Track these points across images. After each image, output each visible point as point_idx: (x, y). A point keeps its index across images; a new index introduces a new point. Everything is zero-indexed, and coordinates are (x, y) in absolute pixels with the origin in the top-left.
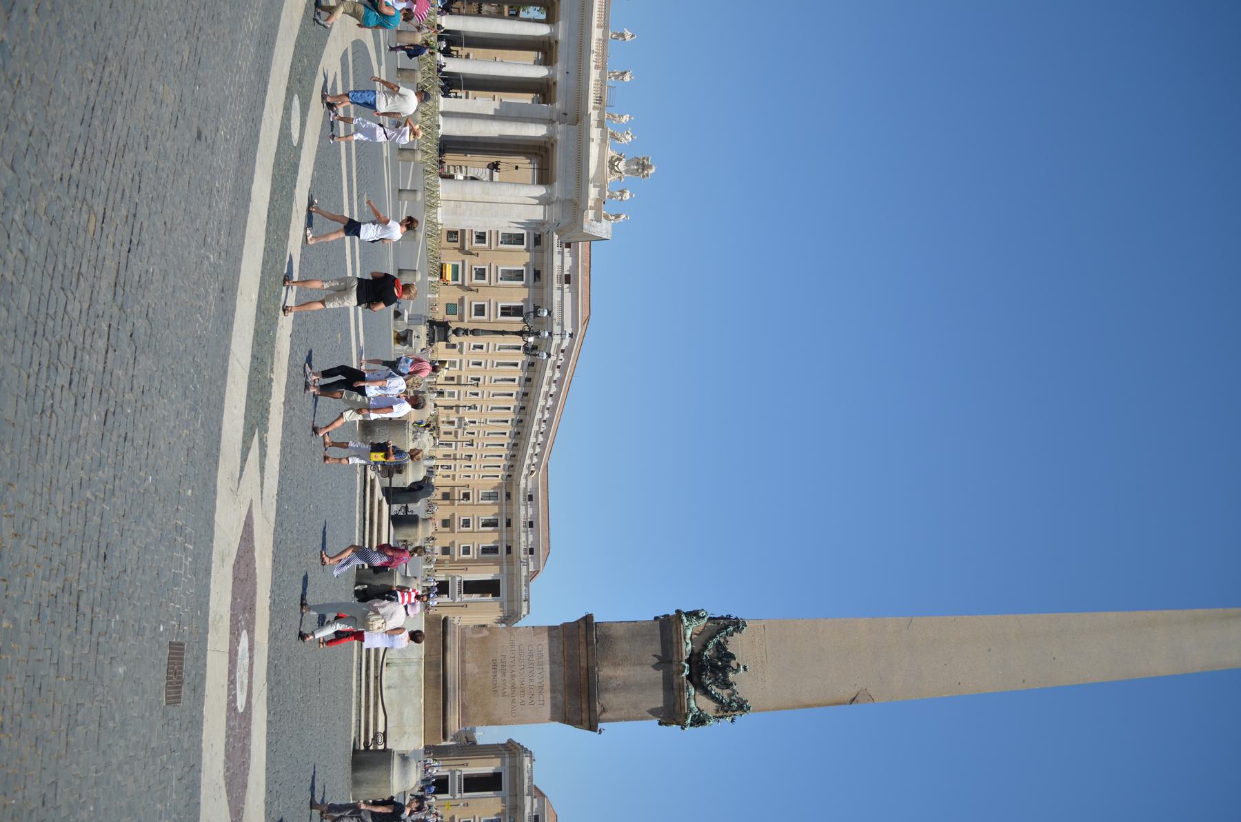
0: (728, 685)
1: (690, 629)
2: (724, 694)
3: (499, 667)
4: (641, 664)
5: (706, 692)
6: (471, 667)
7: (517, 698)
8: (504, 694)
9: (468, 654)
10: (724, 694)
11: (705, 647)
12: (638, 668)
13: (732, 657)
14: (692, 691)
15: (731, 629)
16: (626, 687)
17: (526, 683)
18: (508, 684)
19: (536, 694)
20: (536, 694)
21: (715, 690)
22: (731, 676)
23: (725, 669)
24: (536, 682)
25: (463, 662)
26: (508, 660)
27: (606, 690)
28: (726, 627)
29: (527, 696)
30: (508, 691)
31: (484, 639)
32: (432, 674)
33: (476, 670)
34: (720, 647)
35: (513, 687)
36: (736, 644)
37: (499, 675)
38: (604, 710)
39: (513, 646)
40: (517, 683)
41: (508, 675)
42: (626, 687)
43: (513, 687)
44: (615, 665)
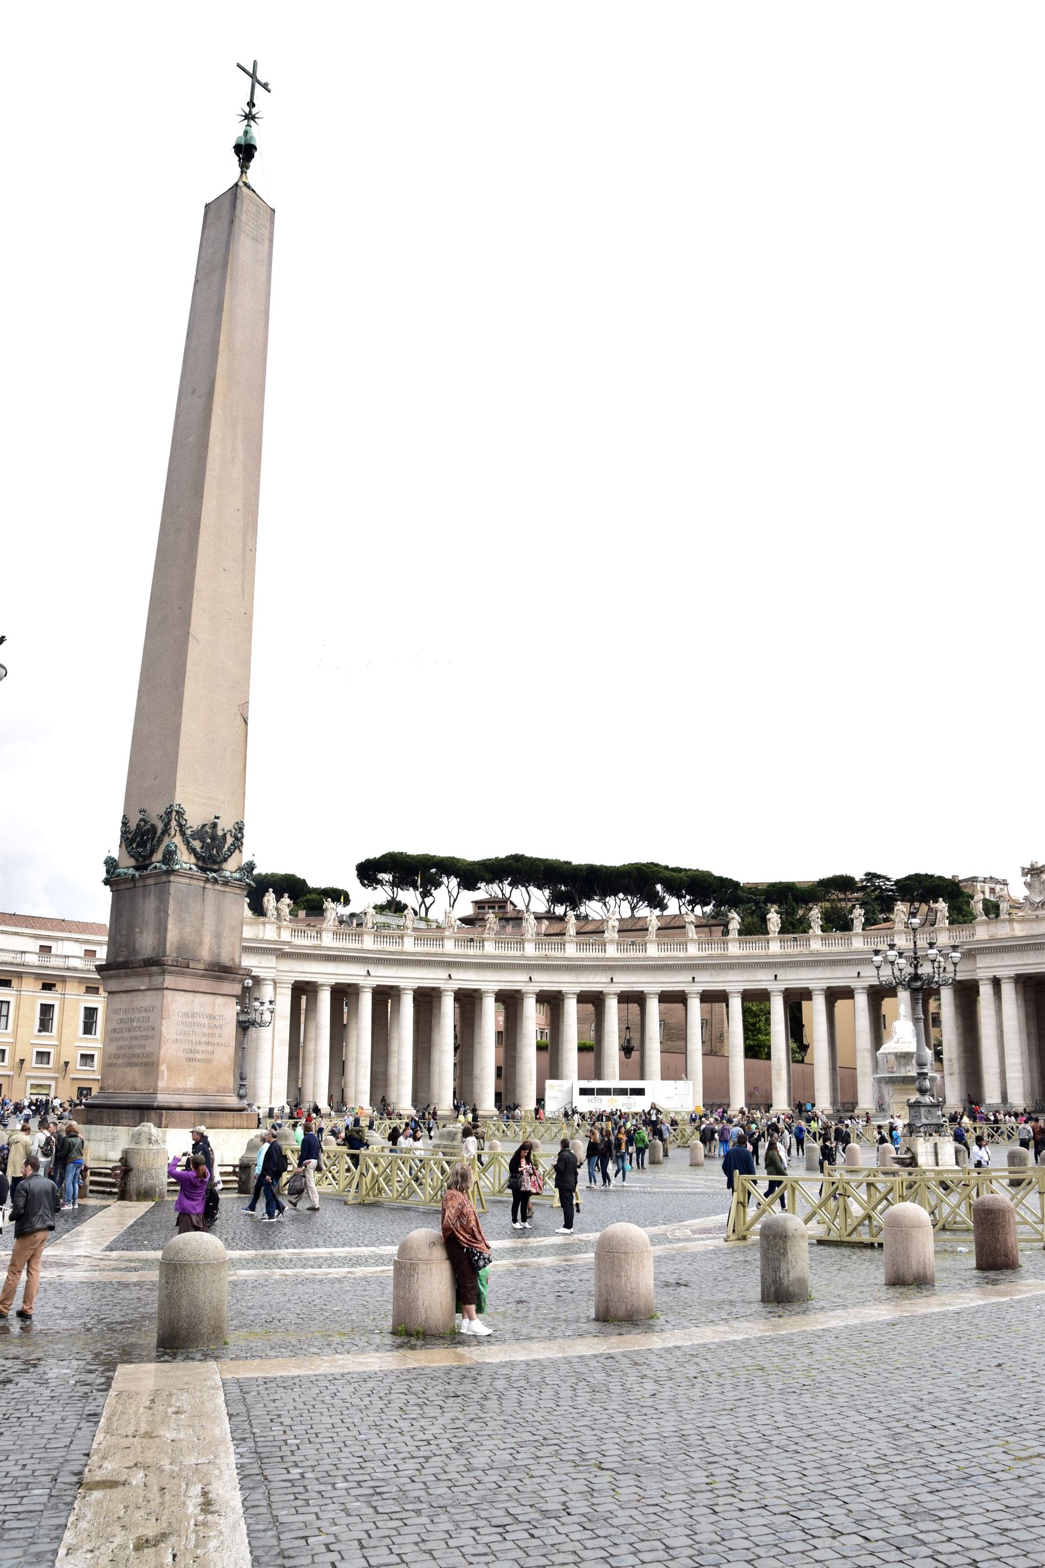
2: (230, 840)
3: (192, 1056)
4: (203, 918)
6: (190, 1083)
7: (216, 1040)
8: (213, 1053)
9: (180, 1085)
10: (230, 840)
12: (206, 921)
13: (204, 826)
16: (218, 936)
17: (206, 1031)
18: (205, 1048)
19: (215, 1022)
20: (215, 1022)
22: (220, 833)
23: (214, 837)
24: (206, 1021)
26: (187, 1046)
27: (219, 955)
29: (217, 1031)
30: (210, 1048)
31: (169, 1069)
33: (192, 1078)
35: (207, 1043)
36: (194, 819)
37: (198, 1056)
38: (233, 959)
39: (176, 1041)
40: (204, 1039)
41: (199, 1048)
42: (218, 936)
43: (207, 1043)
44: (201, 943)
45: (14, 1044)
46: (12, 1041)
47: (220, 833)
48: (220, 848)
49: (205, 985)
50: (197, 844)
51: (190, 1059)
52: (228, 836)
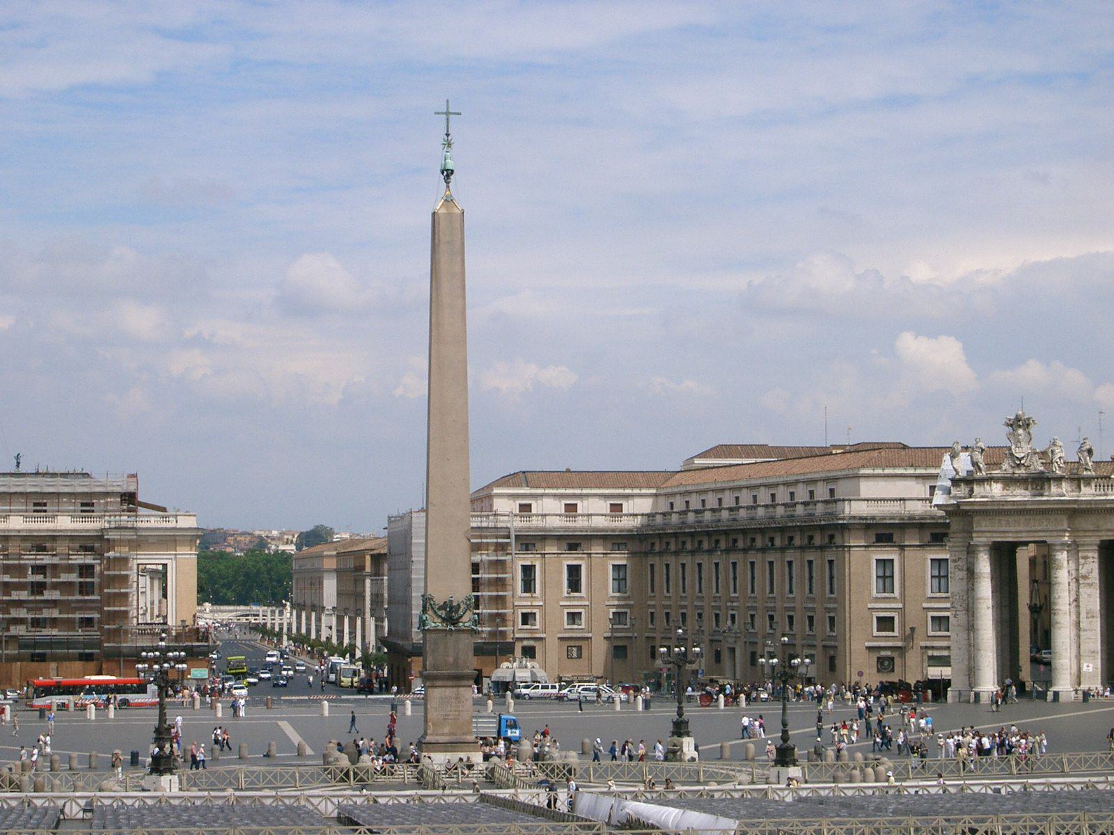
0: (459, 605)
1: (431, 625)
2: (463, 606)
5: (462, 616)
6: (446, 730)
11: (440, 616)
13: (445, 603)
14: (461, 624)
15: (432, 602)
21: (461, 612)
22: (455, 604)
23: (451, 607)
25: (443, 734)
28: (431, 604)
30: (457, 713)
32: (450, 749)
34: (440, 609)
36: (439, 599)
43: (455, 711)
45: (902, 611)
46: (900, 606)
47: (455, 604)
48: (457, 612)
49: (450, 683)
50: (440, 613)
51: (445, 719)
52: (462, 604)
